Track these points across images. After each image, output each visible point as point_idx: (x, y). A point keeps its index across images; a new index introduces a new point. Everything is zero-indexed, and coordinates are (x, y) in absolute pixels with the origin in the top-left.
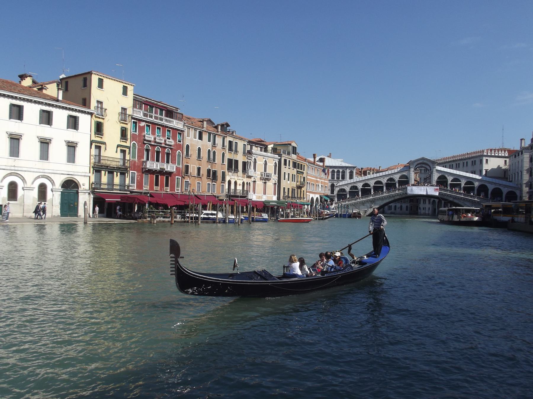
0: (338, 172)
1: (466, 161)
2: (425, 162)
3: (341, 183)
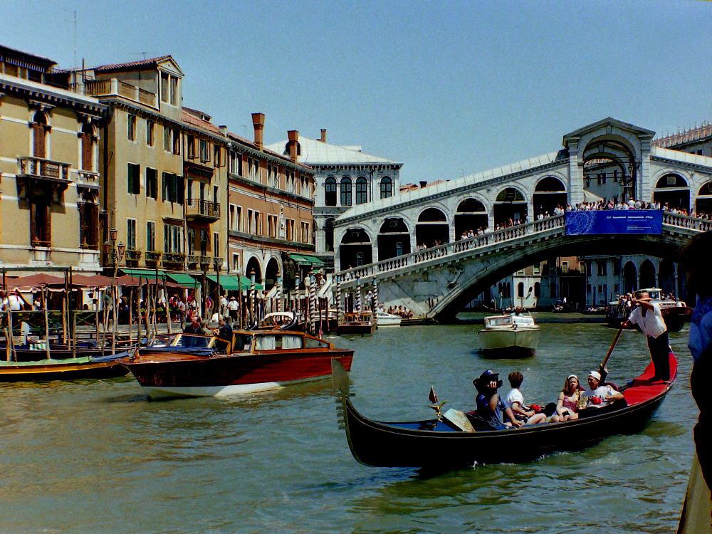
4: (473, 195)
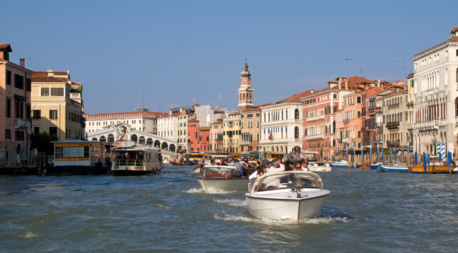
1: (127, 120)
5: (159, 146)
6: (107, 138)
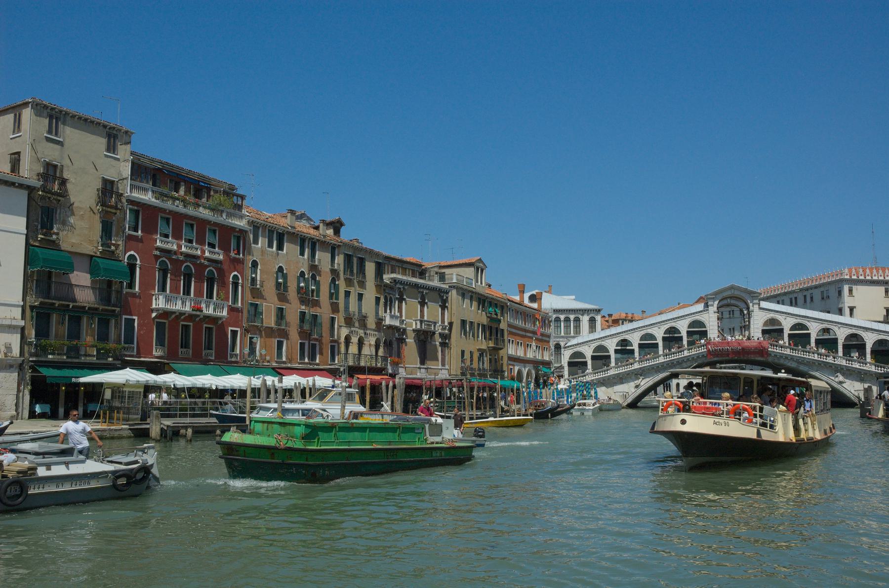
0: (567, 320)
1: (810, 291)
2: (737, 293)
3: (574, 342)
4: (650, 331)
5: (862, 354)
6: (684, 334)
